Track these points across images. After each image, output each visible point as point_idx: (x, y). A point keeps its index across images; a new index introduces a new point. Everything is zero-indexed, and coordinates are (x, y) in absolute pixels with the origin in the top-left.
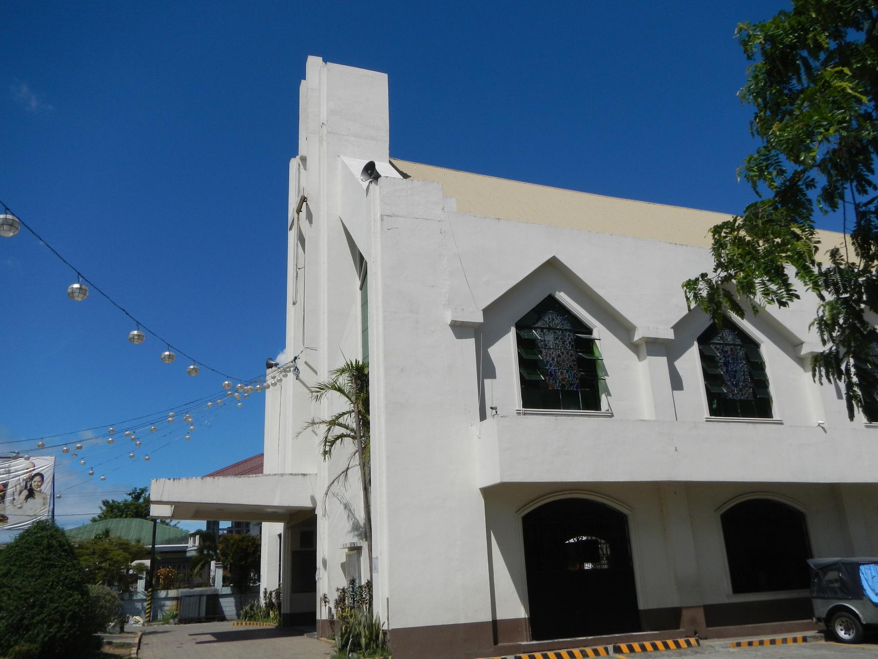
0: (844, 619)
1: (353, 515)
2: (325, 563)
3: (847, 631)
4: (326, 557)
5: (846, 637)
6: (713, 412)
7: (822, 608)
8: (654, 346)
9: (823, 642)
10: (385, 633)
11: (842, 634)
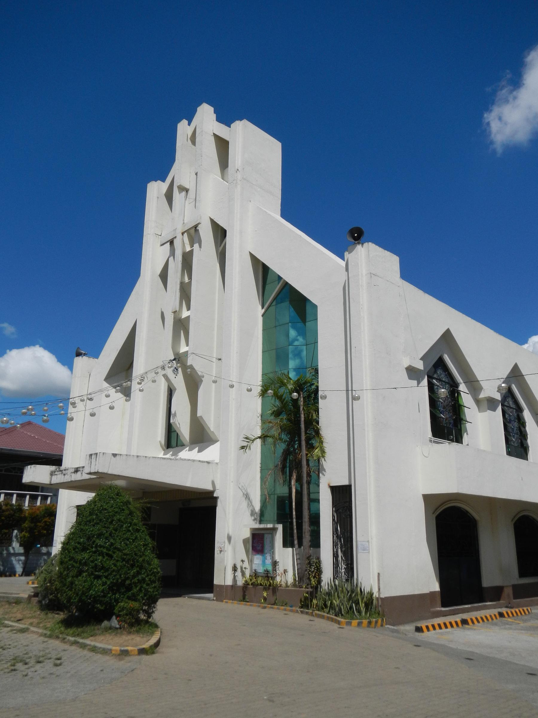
2: (229, 538)
4: (230, 534)
8: (491, 404)
10: (377, 599)
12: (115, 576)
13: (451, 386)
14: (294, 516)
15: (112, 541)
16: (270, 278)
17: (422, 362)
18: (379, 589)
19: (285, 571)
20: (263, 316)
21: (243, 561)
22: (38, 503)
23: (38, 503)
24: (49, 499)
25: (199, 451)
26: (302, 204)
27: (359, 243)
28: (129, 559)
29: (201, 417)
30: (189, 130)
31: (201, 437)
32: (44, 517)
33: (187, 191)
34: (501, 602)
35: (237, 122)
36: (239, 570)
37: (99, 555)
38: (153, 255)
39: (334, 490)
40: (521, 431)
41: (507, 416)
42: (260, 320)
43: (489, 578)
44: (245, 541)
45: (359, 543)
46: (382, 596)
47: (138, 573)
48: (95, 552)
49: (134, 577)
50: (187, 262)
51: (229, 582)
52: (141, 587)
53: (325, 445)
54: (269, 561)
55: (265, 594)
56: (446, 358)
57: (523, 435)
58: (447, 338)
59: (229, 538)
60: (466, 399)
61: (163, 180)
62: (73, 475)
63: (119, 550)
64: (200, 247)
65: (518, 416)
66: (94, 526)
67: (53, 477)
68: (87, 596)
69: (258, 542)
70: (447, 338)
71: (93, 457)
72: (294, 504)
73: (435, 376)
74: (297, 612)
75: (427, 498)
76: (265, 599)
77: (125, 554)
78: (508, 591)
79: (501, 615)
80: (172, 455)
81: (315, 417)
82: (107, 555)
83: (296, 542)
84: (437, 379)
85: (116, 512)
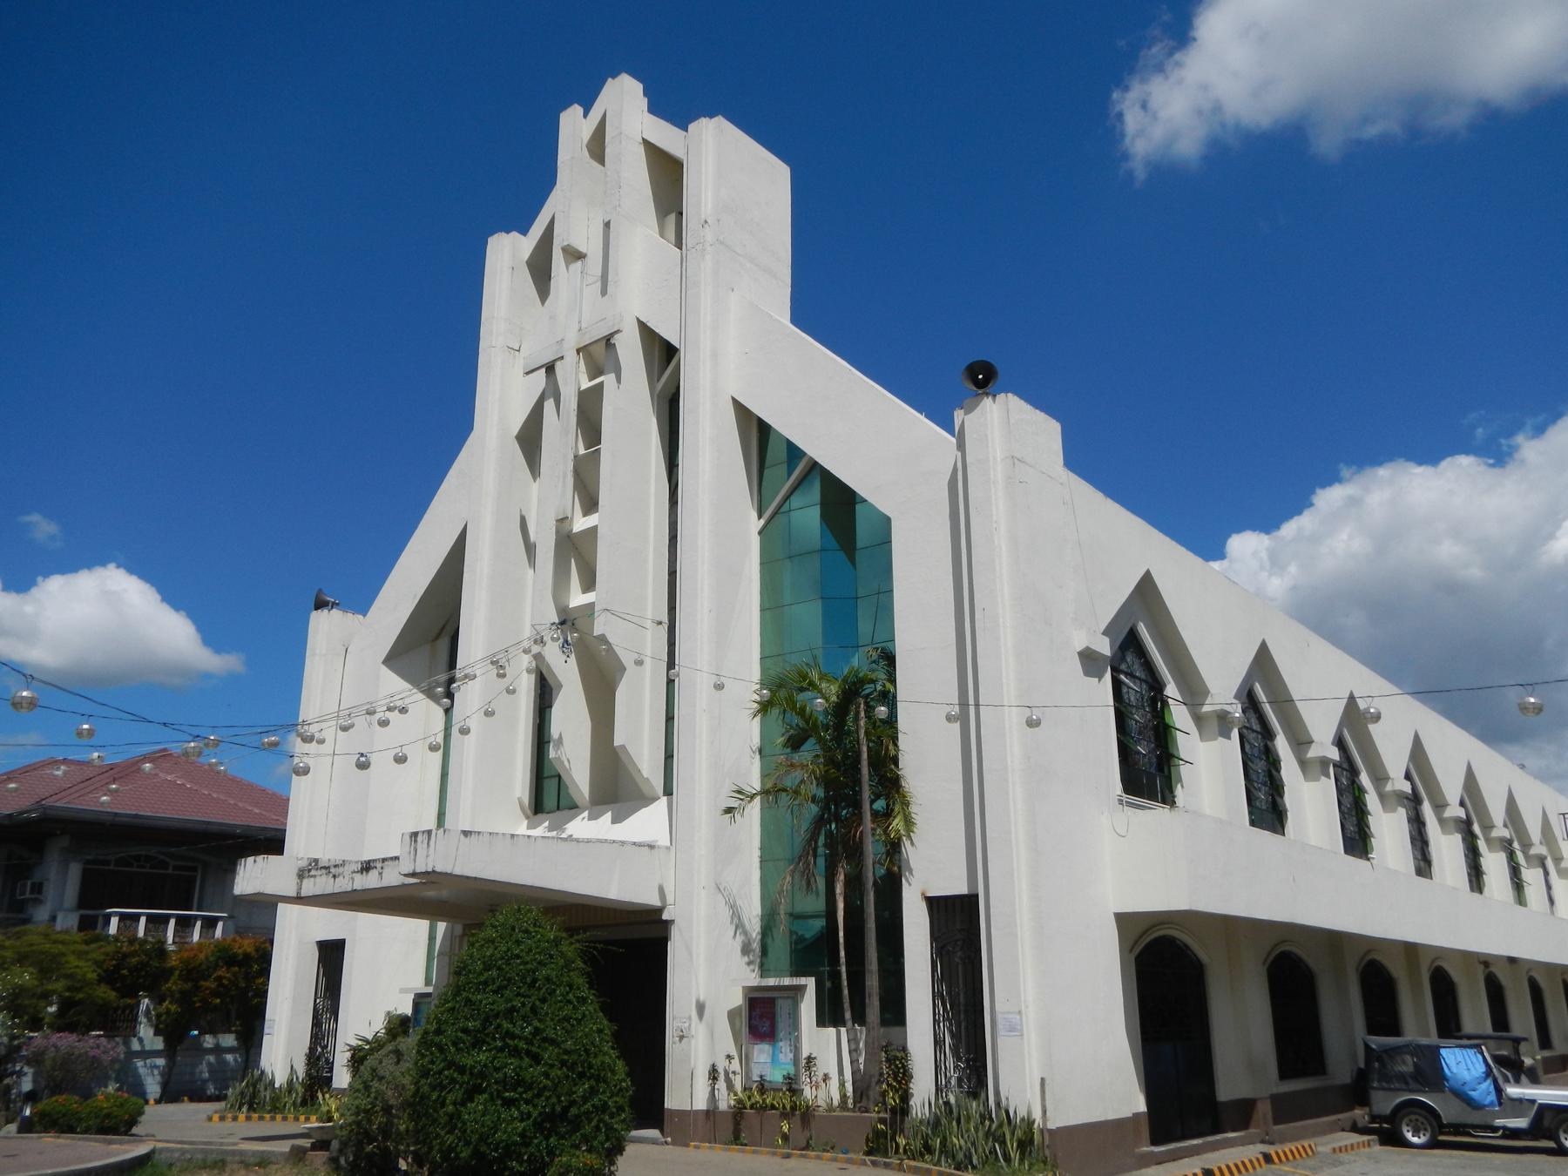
0: (1413, 1117)
1: (743, 927)
2: (701, 1008)
3: (1416, 1133)
5: (1415, 1140)
6: (1253, 823)
7: (1385, 1102)
9: (1377, 1148)
10: (1042, 1131)
11: (1409, 1136)
12: (548, 1099)
13: (1151, 688)
14: (843, 960)
15: (536, 1023)
16: (776, 453)
17: (1107, 640)
18: (1044, 1112)
19: (826, 1078)
20: (760, 533)
21: (729, 1057)
22: (196, 937)
23: (196, 937)
24: (220, 925)
25: (615, 821)
26: (835, 297)
27: (987, 394)
28: (574, 1063)
30: (587, 128)
31: (616, 789)
32: (216, 967)
33: (580, 256)
34: (1252, 1130)
35: (704, 121)
36: (722, 1077)
37: (511, 1056)
38: (502, 393)
39: (938, 907)
40: (1271, 776)
41: (1247, 747)
42: (755, 542)
43: (1231, 1083)
44: (732, 1015)
45: (999, 1017)
46: (1051, 1125)
47: (593, 1091)
48: (501, 1050)
49: (585, 1099)
51: (701, 1104)
52: (600, 1121)
53: (913, 809)
54: (786, 1056)
55: (785, 1129)
56: (1143, 631)
57: (1276, 787)
58: (1146, 590)
59: (701, 1008)
60: (1179, 715)
62: (358, 877)
63: (553, 1042)
64: (619, 380)
65: (1266, 747)
66: (495, 992)
67: (305, 881)
68: (489, 1145)
69: (762, 1017)
70: (1146, 590)
71: (420, 838)
72: (841, 934)
73: (1123, 667)
74: (864, 1163)
75: (1123, 919)
76: (785, 1137)
77: (566, 1052)
78: (1264, 1110)
79: (1268, 1158)
80: (550, 829)
81: (892, 753)
82: (528, 1053)
83: (848, 1015)
84: (1126, 674)
85: (540, 963)
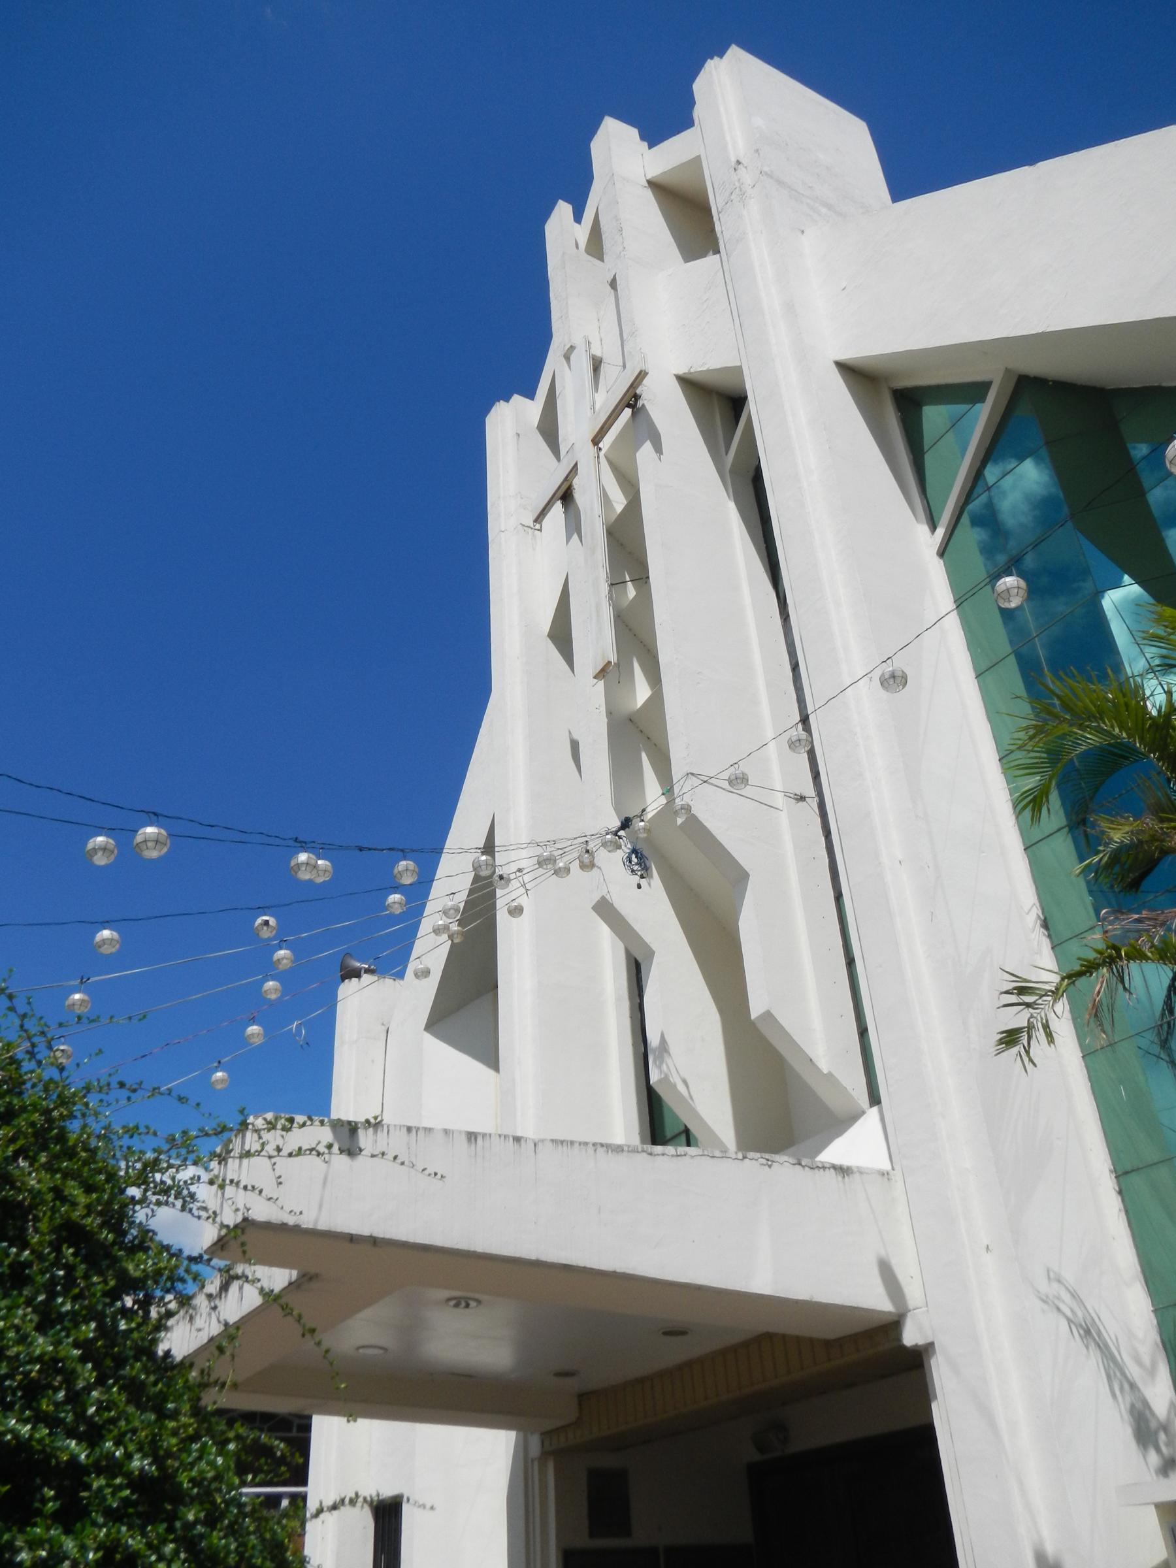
4: (1050, 1549)
20: (942, 553)
29: (768, 1016)
42: (936, 573)
50: (626, 548)
61: (530, 394)
64: (658, 449)
